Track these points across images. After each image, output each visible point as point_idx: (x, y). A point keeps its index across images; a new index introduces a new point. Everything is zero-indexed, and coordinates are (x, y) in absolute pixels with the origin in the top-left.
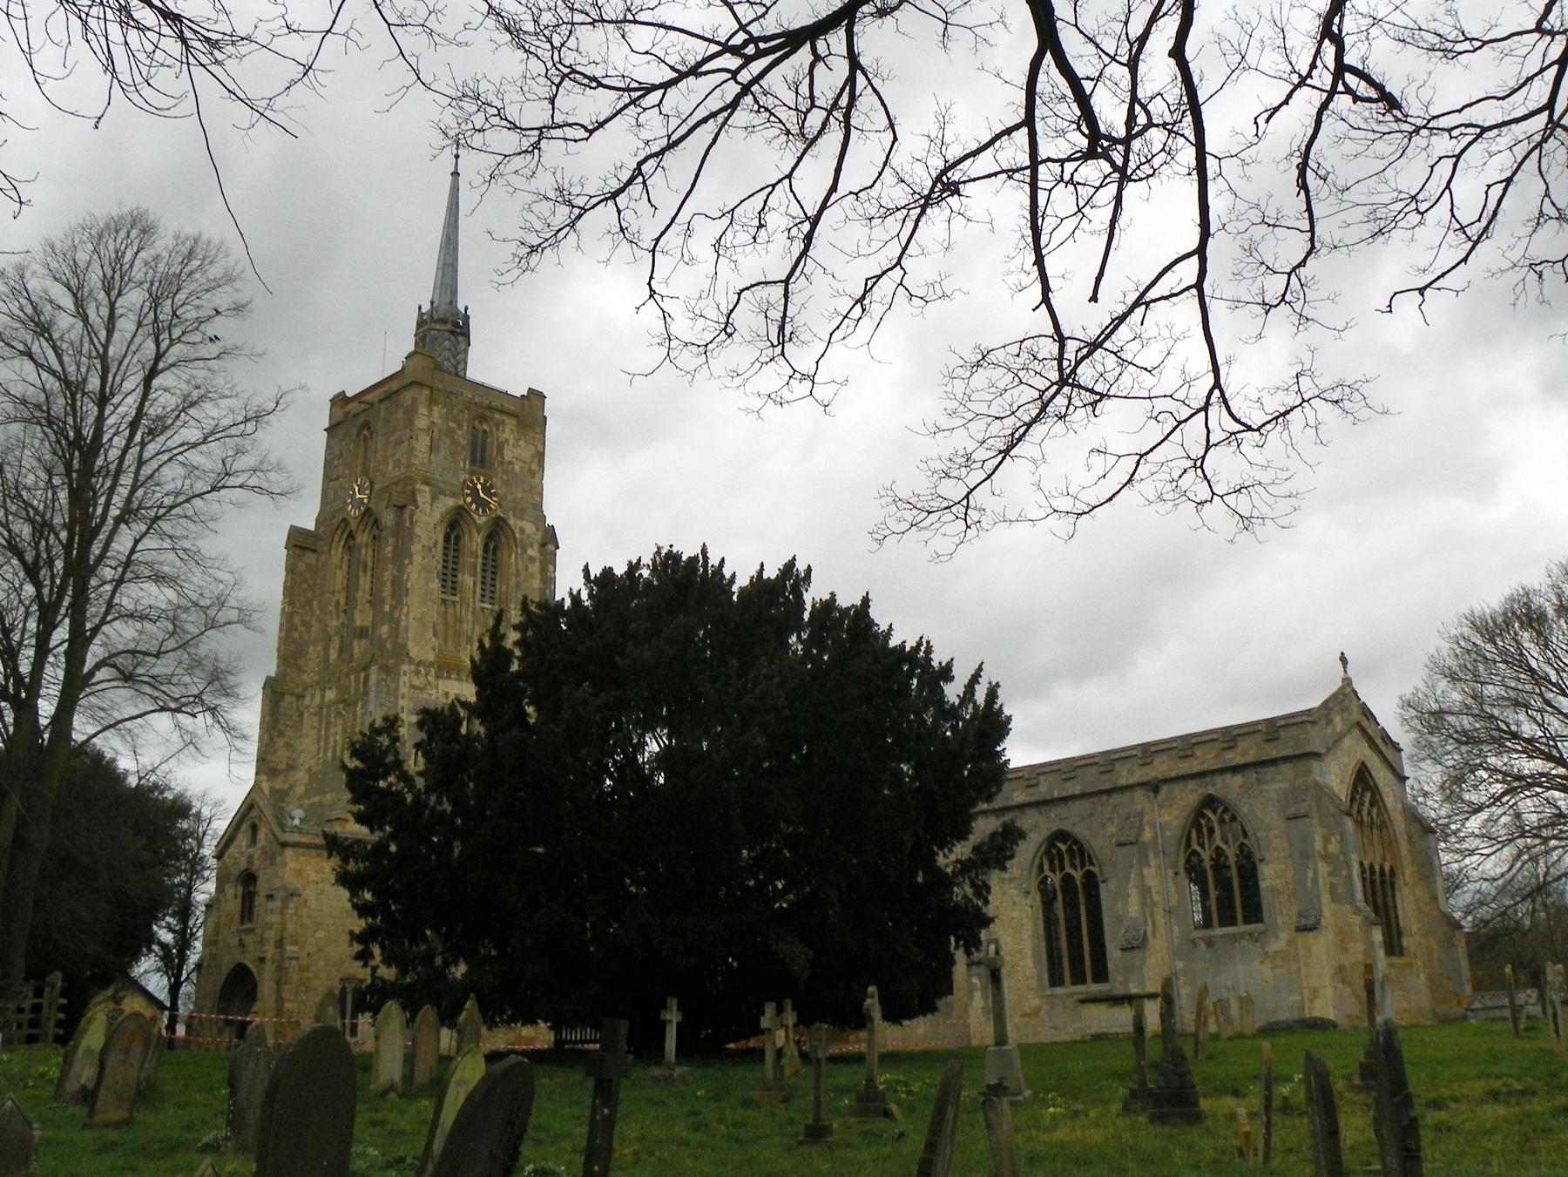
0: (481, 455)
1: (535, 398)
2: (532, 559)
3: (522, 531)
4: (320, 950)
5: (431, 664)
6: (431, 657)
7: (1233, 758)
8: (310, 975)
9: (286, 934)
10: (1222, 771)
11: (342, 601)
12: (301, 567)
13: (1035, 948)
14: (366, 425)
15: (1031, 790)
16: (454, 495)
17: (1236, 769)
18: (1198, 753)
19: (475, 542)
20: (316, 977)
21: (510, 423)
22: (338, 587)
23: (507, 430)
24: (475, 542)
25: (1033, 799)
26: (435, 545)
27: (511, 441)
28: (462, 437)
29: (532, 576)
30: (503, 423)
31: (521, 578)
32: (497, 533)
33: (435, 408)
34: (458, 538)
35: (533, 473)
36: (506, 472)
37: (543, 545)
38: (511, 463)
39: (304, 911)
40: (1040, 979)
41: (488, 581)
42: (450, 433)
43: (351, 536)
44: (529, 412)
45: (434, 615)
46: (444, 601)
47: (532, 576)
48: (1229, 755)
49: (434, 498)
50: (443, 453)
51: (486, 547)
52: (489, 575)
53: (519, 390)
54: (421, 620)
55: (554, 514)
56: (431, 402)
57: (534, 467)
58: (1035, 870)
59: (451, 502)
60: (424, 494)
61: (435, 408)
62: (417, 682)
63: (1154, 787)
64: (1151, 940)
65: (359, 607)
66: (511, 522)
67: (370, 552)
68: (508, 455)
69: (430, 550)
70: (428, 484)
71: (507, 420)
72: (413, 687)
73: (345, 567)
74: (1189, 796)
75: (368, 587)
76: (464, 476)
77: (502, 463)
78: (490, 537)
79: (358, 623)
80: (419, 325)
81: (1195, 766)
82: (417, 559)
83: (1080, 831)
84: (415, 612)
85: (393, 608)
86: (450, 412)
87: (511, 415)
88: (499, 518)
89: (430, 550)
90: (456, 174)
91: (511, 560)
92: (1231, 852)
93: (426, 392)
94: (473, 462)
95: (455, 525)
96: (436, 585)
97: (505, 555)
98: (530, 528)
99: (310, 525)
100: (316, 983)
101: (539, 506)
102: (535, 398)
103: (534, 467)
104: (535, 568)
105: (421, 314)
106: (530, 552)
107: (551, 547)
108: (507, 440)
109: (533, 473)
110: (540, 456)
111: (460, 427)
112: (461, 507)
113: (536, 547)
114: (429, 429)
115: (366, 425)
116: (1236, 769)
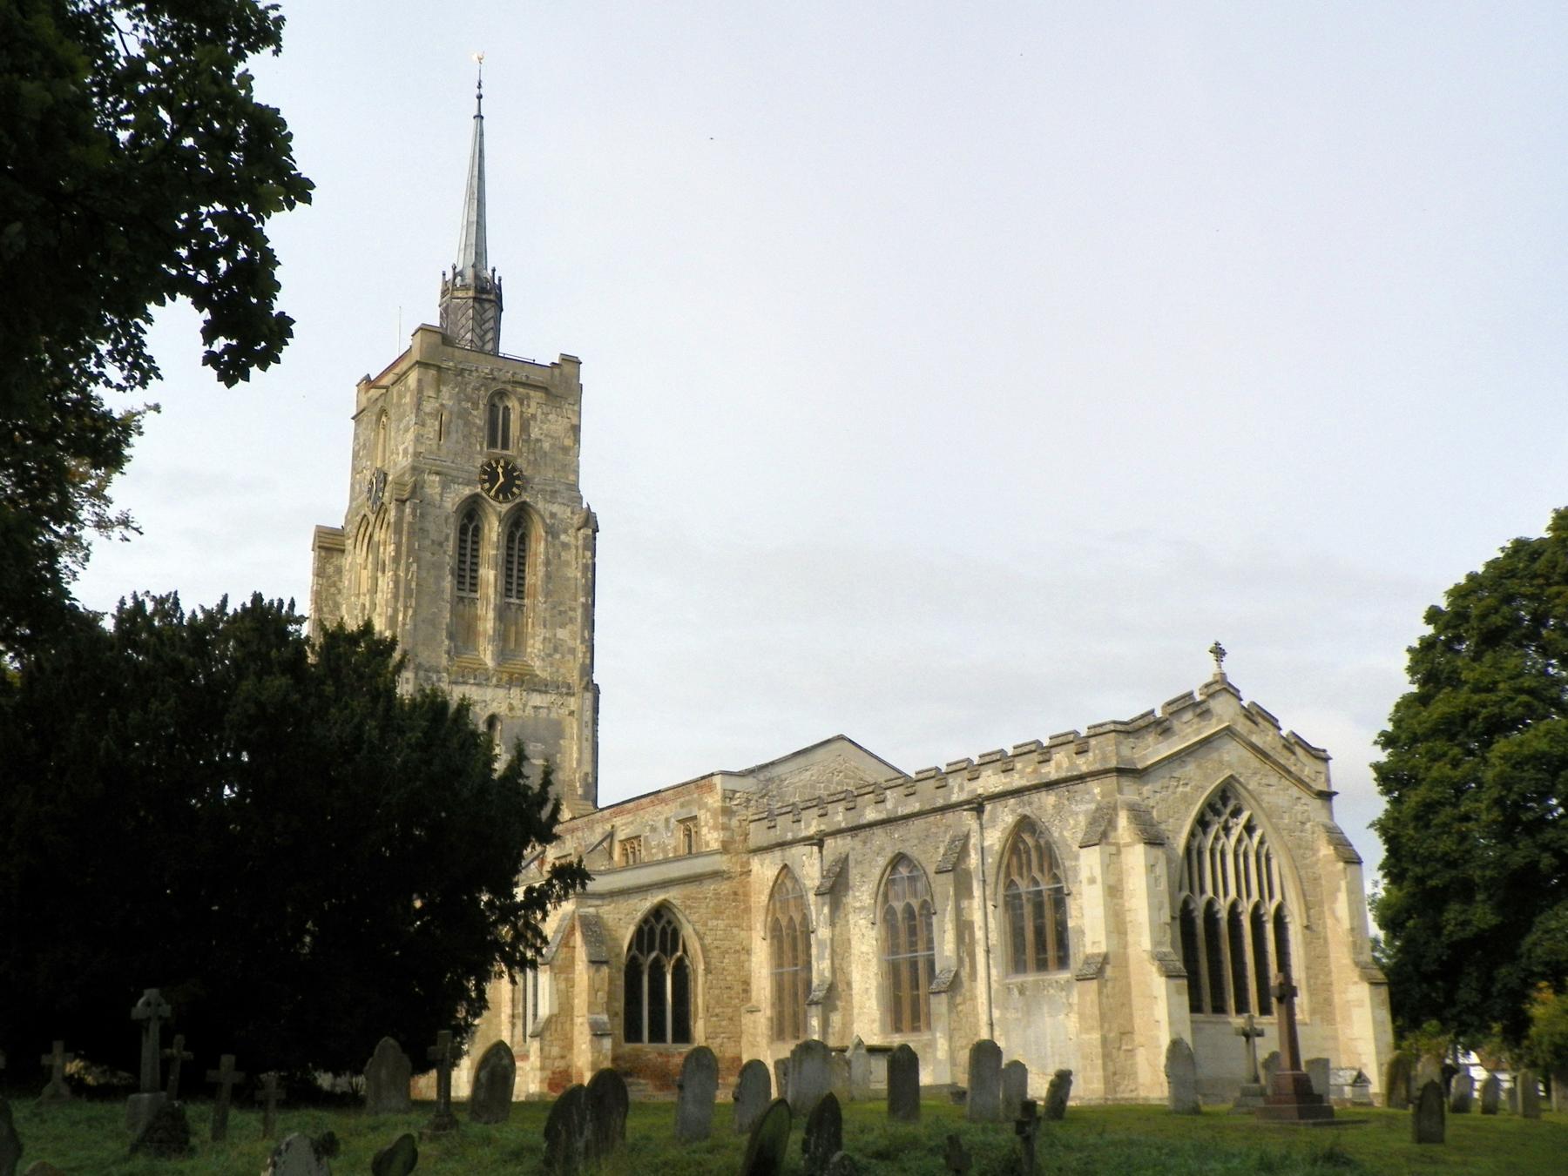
2: (565, 546)
3: (553, 515)
7: (1051, 771)
10: (1036, 788)
13: (879, 986)
14: (383, 412)
15: (880, 806)
16: (467, 484)
17: (1050, 785)
18: (1019, 766)
21: (537, 396)
22: (364, 589)
23: (533, 404)
25: (883, 816)
27: (539, 416)
28: (479, 417)
29: (567, 564)
30: (528, 397)
33: (444, 389)
35: (565, 450)
36: (534, 452)
38: (538, 440)
40: (883, 1024)
42: (463, 415)
44: (560, 383)
46: (461, 599)
48: (1045, 769)
49: (445, 486)
50: (454, 436)
51: (510, 538)
53: (547, 357)
55: (592, 492)
56: (439, 383)
57: (568, 442)
58: (880, 898)
59: (467, 491)
61: (444, 389)
63: (977, 805)
64: (966, 984)
66: (540, 505)
68: (535, 433)
69: (441, 544)
70: (437, 473)
71: (532, 393)
73: (370, 567)
74: (1006, 815)
76: (480, 461)
77: (527, 441)
80: (444, 294)
81: (1016, 781)
83: (913, 851)
86: (463, 391)
87: (535, 387)
88: (524, 503)
90: (479, 117)
93: (433, 372)
94: (492, 443)
95: (470, 514)
98: (562, 511)
99: (337, 522)
101: (574, 487)
105: (446, 283)
106: (563, 537)
108: (534, 416)
110: (576, 429)
111: (475, 405)
112: (477, 495)
113: (572, 531)
114: (438, 414)
115: (383, 412)
116: (1050, 785)
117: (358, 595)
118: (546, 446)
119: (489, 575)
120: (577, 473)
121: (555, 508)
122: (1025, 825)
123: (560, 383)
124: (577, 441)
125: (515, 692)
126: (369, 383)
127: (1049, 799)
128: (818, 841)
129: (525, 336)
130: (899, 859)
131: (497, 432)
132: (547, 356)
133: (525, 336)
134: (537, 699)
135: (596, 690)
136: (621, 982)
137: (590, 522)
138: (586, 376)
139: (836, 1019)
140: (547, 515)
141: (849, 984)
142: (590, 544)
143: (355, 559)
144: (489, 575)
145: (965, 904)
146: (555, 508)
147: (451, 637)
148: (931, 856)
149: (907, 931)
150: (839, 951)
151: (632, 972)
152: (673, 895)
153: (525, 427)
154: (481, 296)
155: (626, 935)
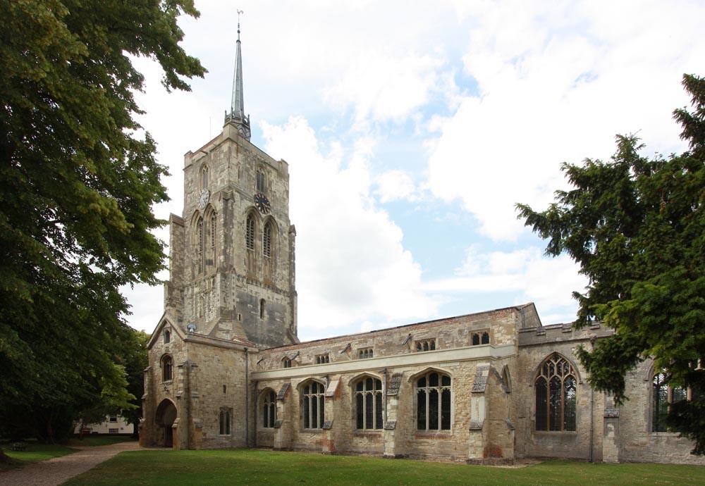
3: (281, 225)
4: (209, 394)
5: (244, 277)
6: (244, 274)
8: (205, 405)
9: (191, 386)
11: (199, 250)
12: (178, 233)
20: (208, 407)
26: (243, 222)
31: (281, 246)
32: (270, 223)
34: (253, 223)
37: (290, 233)
39: (199, 375)
41: (267, 245)
43: (201, 219)
45: (244, 255)
47: (286, 246)
52: (267, 243)
54: (239, 256)
57: (285, 197)
62: (238, 284)
65: (208, 251)
66: (276, 219)
67: (211, 225)
72: (237, 286)
73: (199, 234)
75: (211, 242)
78: (267, 225)
79: (208, 258)
82: (236, 227)
84: (236, 252)
85: (226, 248)
88: (271, 216)
89: (241, 224)
91: (276, 237)
95: (251, 216)
97: (274, 235)
98: (284, 224)
100: (207, 409)
101: (287, 216)
103: (285, 197)
104: (287, 243)
106: (284, 234)
107: (293, 234)
109: (285, 200)
110: (287, 192)
113: (287, 233)
117: (194, 245)
118: (278, 195)
119: (259, 243)
120: (288, 210)
121: (281, 222)
124: (288, 197)
131: (261, 185)
137: (292, 230)
140: (279, 224)
142: (292, 240)
146: (281, 222)
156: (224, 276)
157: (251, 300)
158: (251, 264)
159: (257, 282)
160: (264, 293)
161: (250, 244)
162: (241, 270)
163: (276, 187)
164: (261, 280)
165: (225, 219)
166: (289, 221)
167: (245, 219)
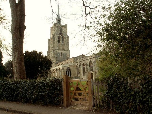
0: (61, 30)
1: (66, 24)
2: (66, 39)
19: (61, 39)
21: (64, 27)
24: (61, 39)
32: (63, 38)
44: (66, 26)
59: (58, 35)
60: (56, 35)
63: (88, 60)
91: (64, 39)
92: (91, 65)
95: (59, 37)
96: (57, 43)
98: (66, 36)
99: (50, 38)
101: (67, 34)
102: (66, 24)
104: (67, 40)
110: (67, 30)
119: (61, 42)
122: (90, 61)
123: (66, 26)
125: (63, 51)
126: (51, 27)
127: (92, 59)
128: (79, 62)
129: (62, 23)
130: (84, 64)
132: (64, 24)
133: (62, 23)
134: (64, 51)
135: (69, 50)
136: (66, 73)
137: (68, 37)
138: (68, 26)
139: (80, 75)
141: (81, 72)
142: (68, 39)
143: (51, 41)
144: (61, 42)
145: (87, 67)
147: (58, 47)
148: (85, 63)
149: (84, 68)
150: (80, 70)
151: (67, 72)
152: (69, 66)
153: (63, 30)
154: (59, 20)
155: (66, 69)
156: (53, 50)
157: (59, 53)
158: (59, 46)
159: (60, 50)
160: (62, 51)
161: (59, 42)
162: (57, 48)
163: (64, 29)
164: (61, 49)
165: (53, 40)
166: (67, 35)
167: (57, 38)
